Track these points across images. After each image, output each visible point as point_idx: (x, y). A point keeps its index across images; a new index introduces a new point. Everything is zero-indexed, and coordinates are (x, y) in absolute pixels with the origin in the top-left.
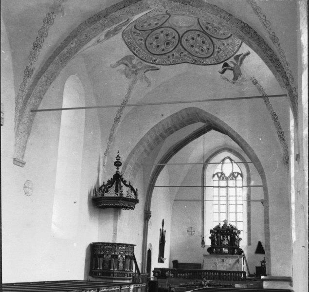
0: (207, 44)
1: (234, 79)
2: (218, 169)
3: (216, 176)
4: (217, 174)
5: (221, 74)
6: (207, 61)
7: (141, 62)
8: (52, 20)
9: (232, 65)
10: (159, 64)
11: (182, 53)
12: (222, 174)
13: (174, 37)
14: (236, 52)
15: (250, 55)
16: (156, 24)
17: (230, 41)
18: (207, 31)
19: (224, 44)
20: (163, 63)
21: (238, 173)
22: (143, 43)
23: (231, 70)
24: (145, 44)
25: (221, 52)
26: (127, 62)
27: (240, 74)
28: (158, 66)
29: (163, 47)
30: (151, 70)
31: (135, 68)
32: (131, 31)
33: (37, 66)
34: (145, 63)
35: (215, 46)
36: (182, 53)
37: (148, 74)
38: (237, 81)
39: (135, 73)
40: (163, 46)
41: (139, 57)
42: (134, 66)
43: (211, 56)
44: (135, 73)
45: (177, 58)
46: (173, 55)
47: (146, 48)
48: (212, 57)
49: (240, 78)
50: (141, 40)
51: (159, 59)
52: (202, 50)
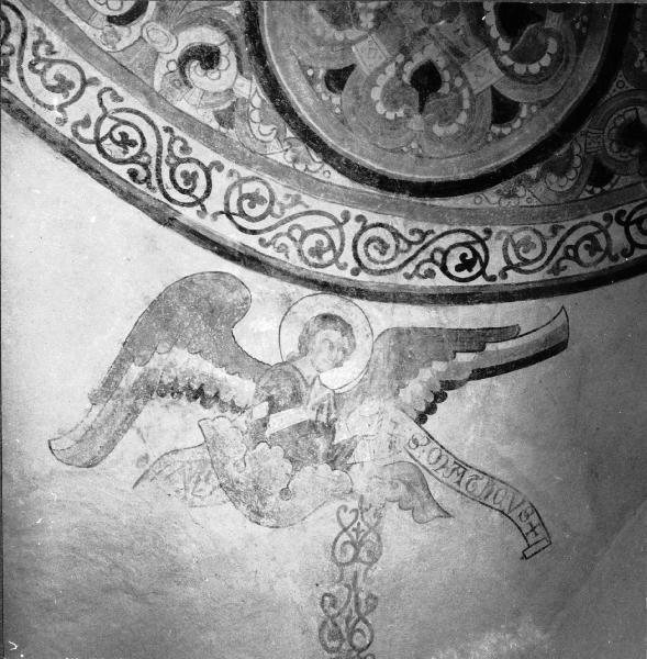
7: (325, 317)
20: (573, 270)
22: (250, 89)
24: (273, 89)
26: (185, 362)
30: (480, 374)
31: (297, 398)
40: (484, 59)
41: (284, 274)
42: (283, 383)
47: (308, 136)
50: (209, 58)
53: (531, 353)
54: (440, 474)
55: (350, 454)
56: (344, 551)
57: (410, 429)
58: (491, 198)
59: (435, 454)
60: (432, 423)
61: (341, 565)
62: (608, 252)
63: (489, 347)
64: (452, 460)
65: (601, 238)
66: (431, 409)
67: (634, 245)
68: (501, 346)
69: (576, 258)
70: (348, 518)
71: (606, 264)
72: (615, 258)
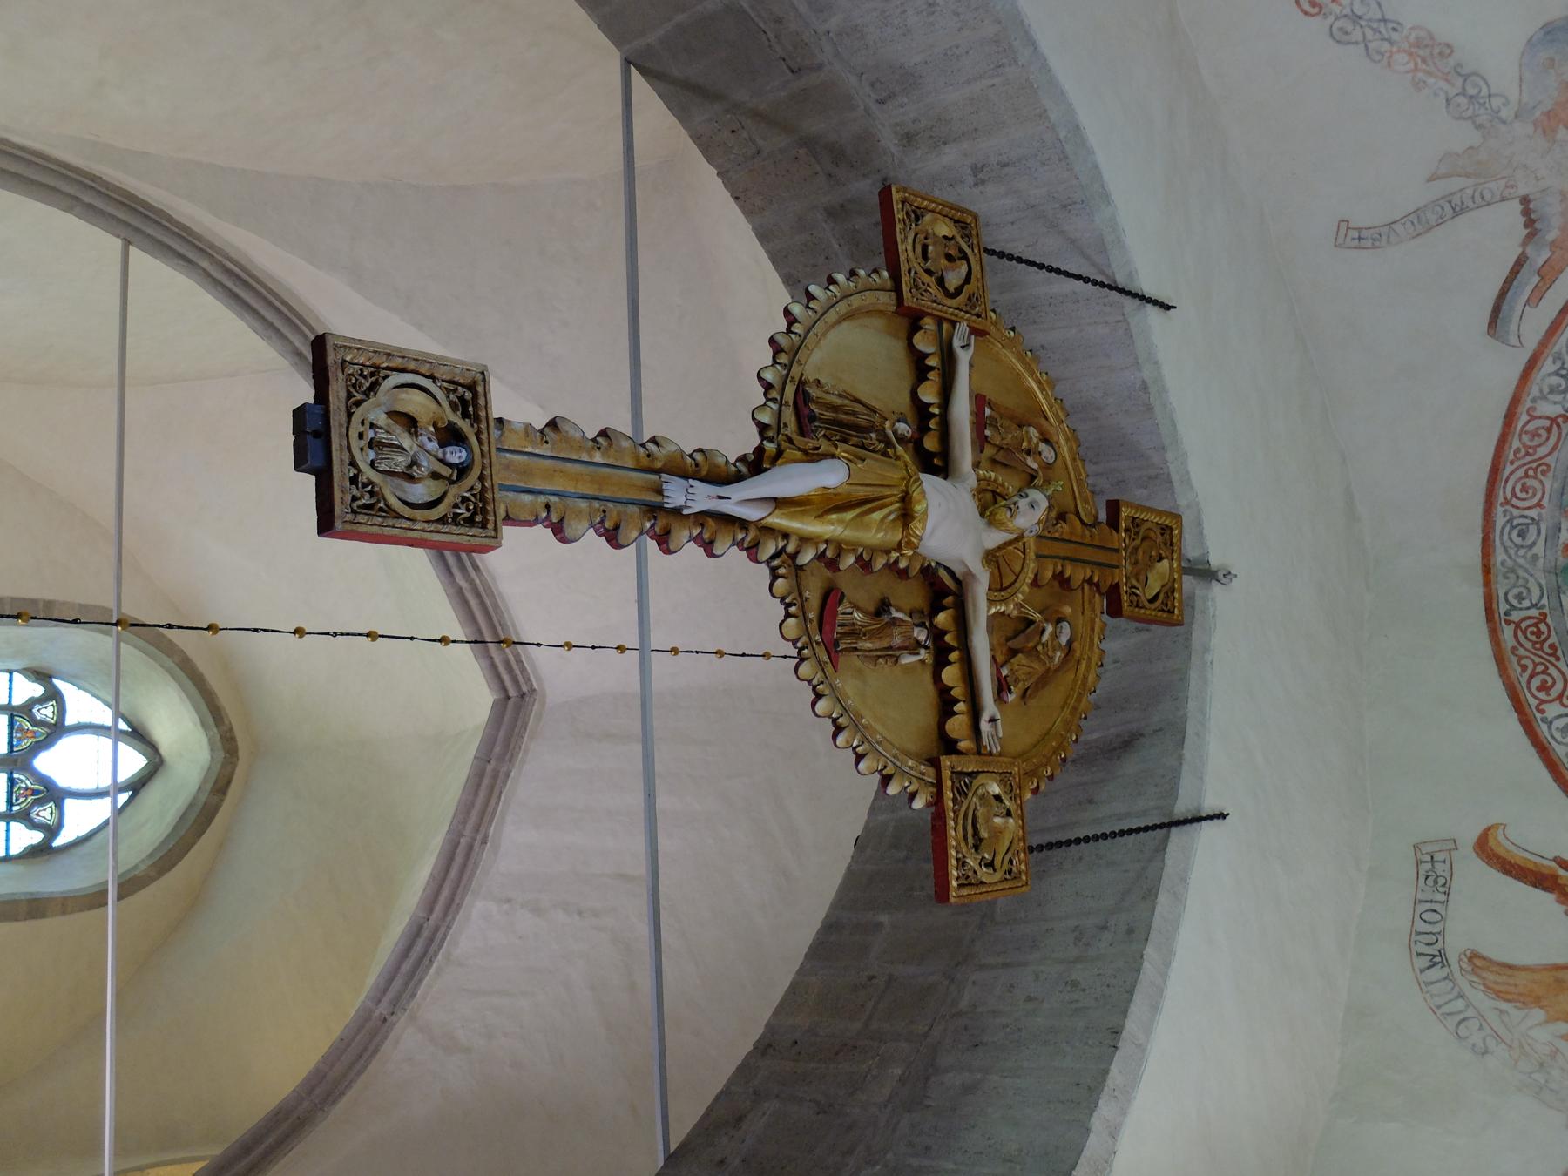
1: (1474, 958)
2: (82, 705)
3: (37, 690)
4: (53, 695)
5: (1469, 836)
12: (58, 729)
20: (1548, 366)
21: (52, 831)
28: (1532, 323)
30: (1520, 263)
37: (1493, 238)
38: (1479, 997)
53: (1505, 307)
54: (1469, 192)
55: (1544, 132)
56: (1475, 85)
57: (1523, 190)
59: (1488, 196)
60: (1516, 206)
61: (1466, 77)
62: (1544, 398)
63: (1536, 279)
64: (1471, 205)
65: (1558, 398)
66: (1526, 212)
67: (1533, 418)
68: (1529, 289)
69: (1557, 373)
70: (1496, 102)
71: (1535, 392)
72: (1534, 400)
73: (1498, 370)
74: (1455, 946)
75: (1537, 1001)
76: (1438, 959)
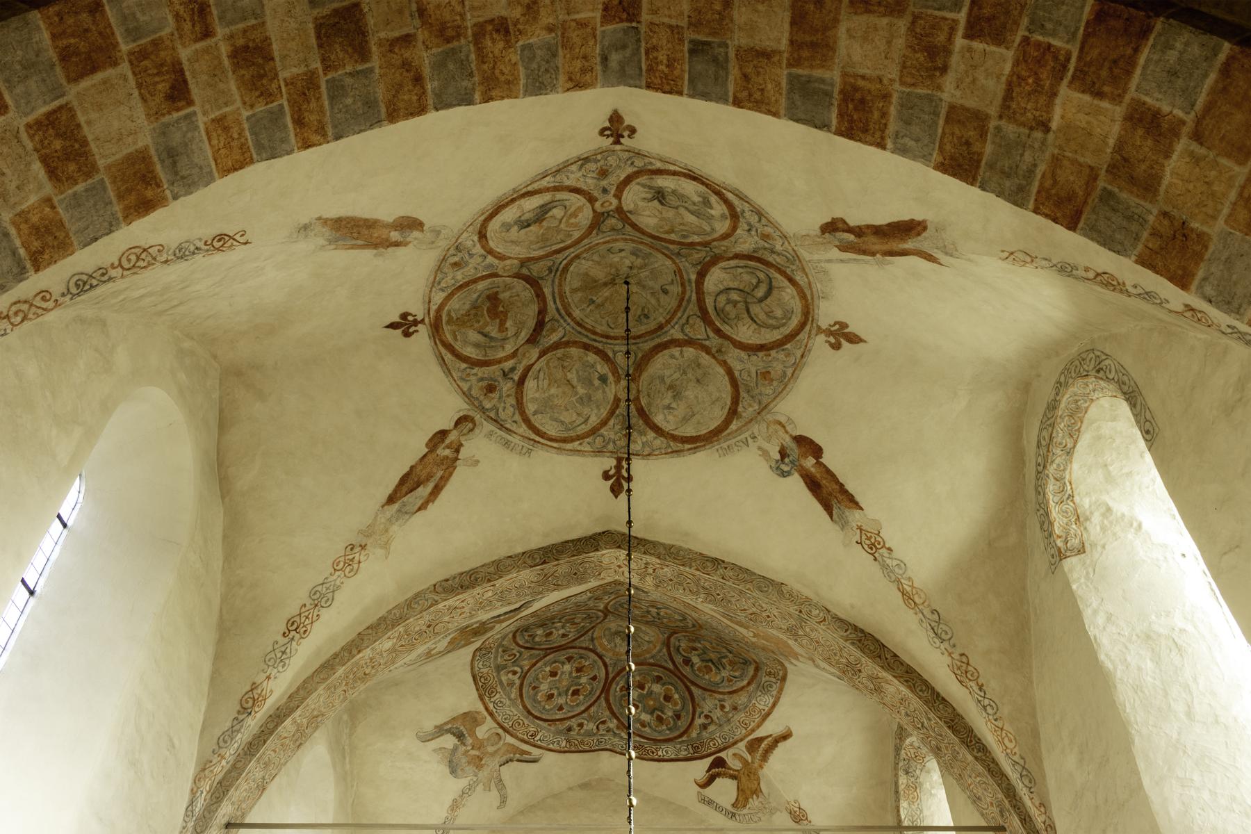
0: (676, 704)
6: (668, 750)
8: (356, 566)
9: (734, 764)
10: (540, 747)
11: (603, 722)
13: (594, 678)
14: (753, 730)
15: (790, 741)
16: (564, 635)
17: (742, 699)
18: (686, 670)
19: (723, 707)
22: (518, 682)
23: (733, 777)
24: (522, 685)
25: (712, 728)
27: (757, 792)
28: (536, 752)
29: (561, 701)
32: (500, 645)
33: (278, 687)
34: (509, 739)
35: (699, 710)
36: (603, 722)
38: (745, 811)
39: (478, 762)
42: (479, 745)
43: (681, 736)
44: (478, 762)
45: (589, 734)
46: (581, 725)
47: (521, 695)
48: (684, 738)
49: (754, 803)
50: (515, 673)
51: (545, 734)
52: (660, 719)
58: (545, 725)
73: (549, 757)
74: (730, 808)
75: (747, 799)
76: (733, 815)
